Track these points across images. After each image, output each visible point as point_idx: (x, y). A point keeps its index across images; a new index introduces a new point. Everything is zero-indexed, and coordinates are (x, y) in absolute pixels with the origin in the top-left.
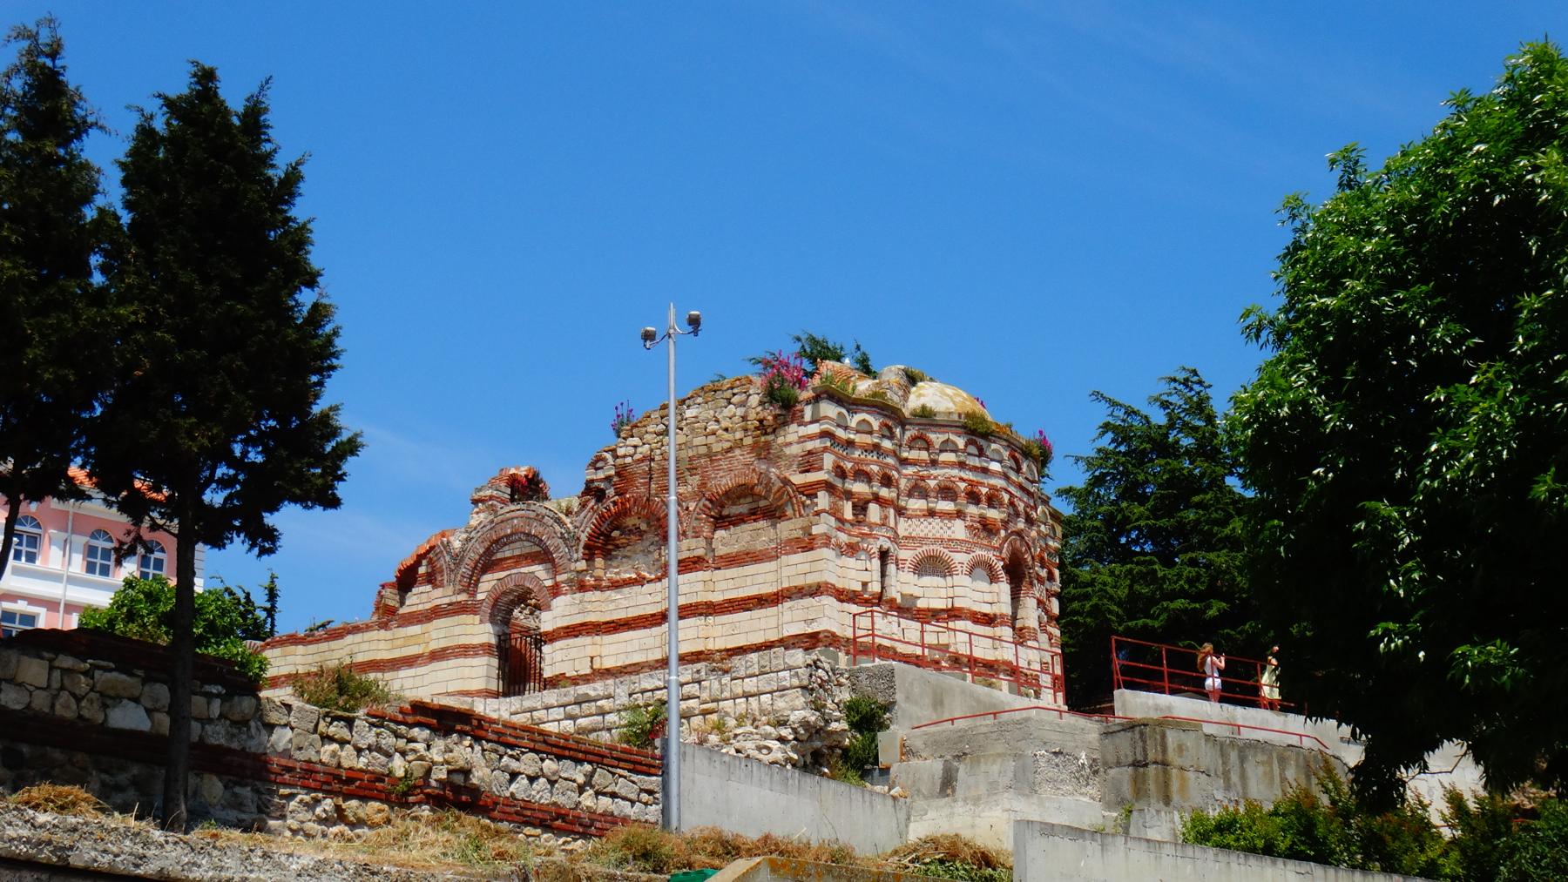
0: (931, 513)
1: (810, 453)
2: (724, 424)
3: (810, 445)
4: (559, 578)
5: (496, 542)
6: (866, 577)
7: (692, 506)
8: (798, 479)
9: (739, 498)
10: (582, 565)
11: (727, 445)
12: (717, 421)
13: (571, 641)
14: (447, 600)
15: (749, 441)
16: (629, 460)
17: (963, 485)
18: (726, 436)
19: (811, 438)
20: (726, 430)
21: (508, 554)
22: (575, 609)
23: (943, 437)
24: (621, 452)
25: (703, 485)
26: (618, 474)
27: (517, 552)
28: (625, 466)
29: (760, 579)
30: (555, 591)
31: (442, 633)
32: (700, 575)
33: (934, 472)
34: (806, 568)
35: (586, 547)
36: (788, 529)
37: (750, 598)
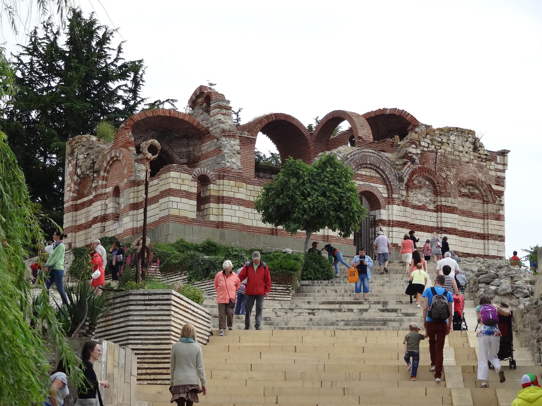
1: (498, 177)
2: (466, 149)
3: (499, 174)
7: (452, 183)
8: (495, 187)
10: (404, 193)
11: (467, 160)
12: (463, 147)
13: (400, 229)
16: (426, 149)
18: (466, 155)
19: (500, 171)
20: (466, 152)
21: (364, 173)
24: (423, 143)
26: (421, 154)
27: (368, 174)
29: (476, 225)
30: (390, 201)
32: (457, 216)
34: (497, 227)
35: (406, 184)
36: (491, 208)
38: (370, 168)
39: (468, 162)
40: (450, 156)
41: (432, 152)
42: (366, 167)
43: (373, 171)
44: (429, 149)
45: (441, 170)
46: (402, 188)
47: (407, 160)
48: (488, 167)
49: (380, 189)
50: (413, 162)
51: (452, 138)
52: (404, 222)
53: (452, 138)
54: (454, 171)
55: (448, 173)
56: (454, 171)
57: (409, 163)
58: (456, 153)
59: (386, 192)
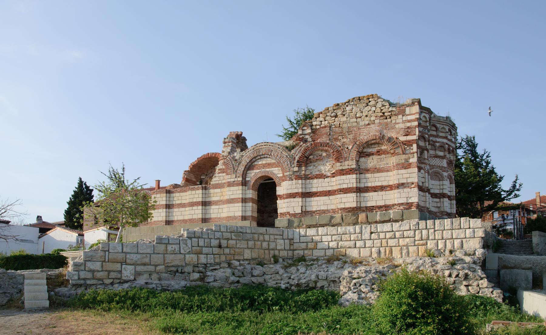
0: (436, 156)
4: (285, 174)
5: (255, 157)
6: (423, 180)
8: (403, 139)
9: (372, 144)
10: (296, 169)
11: (367, 123)
13: (292, 200)
14: (233, 180)
15: (377, 121)
17: (447, 146)
21: (260, 163)
22: (294, 186)
23: (442, 126)
24: (314, 123)
25: (355, 138)
28: (316, 129)
29: (383, 179)
30: (284, 179)
31: (231, 193)
33: (438, 140)
34: (408, 175)
35: (298, 162)
37: (377, 187)
38: (264, 157)
39: (369, 124)
40: (345, 125)
41: (325, 127)
42: (261, 158)
43: (268, 159)
44: (322, 126)
45: (337, 139)
46: (293, 166)
47: (298, 142)
48: (393, 122)
49: (274, 172)
50: (306, 141)
51: (347, 108)
52: (296, 193)
53: (347, 108)
54: (351, 136)
55: (345, 140)
56: (351, 136)
57: (302, 143)
58: (355, 120)
59: (281, 172)
